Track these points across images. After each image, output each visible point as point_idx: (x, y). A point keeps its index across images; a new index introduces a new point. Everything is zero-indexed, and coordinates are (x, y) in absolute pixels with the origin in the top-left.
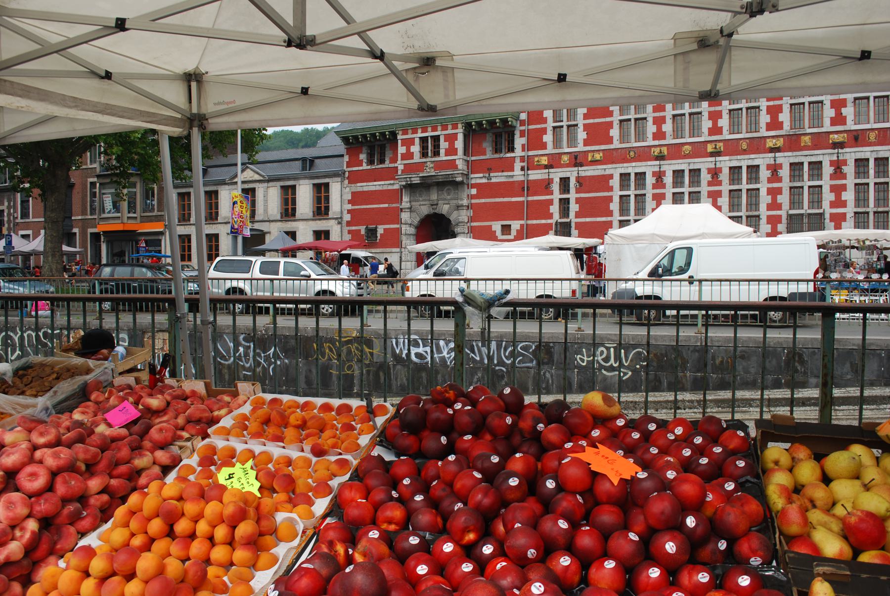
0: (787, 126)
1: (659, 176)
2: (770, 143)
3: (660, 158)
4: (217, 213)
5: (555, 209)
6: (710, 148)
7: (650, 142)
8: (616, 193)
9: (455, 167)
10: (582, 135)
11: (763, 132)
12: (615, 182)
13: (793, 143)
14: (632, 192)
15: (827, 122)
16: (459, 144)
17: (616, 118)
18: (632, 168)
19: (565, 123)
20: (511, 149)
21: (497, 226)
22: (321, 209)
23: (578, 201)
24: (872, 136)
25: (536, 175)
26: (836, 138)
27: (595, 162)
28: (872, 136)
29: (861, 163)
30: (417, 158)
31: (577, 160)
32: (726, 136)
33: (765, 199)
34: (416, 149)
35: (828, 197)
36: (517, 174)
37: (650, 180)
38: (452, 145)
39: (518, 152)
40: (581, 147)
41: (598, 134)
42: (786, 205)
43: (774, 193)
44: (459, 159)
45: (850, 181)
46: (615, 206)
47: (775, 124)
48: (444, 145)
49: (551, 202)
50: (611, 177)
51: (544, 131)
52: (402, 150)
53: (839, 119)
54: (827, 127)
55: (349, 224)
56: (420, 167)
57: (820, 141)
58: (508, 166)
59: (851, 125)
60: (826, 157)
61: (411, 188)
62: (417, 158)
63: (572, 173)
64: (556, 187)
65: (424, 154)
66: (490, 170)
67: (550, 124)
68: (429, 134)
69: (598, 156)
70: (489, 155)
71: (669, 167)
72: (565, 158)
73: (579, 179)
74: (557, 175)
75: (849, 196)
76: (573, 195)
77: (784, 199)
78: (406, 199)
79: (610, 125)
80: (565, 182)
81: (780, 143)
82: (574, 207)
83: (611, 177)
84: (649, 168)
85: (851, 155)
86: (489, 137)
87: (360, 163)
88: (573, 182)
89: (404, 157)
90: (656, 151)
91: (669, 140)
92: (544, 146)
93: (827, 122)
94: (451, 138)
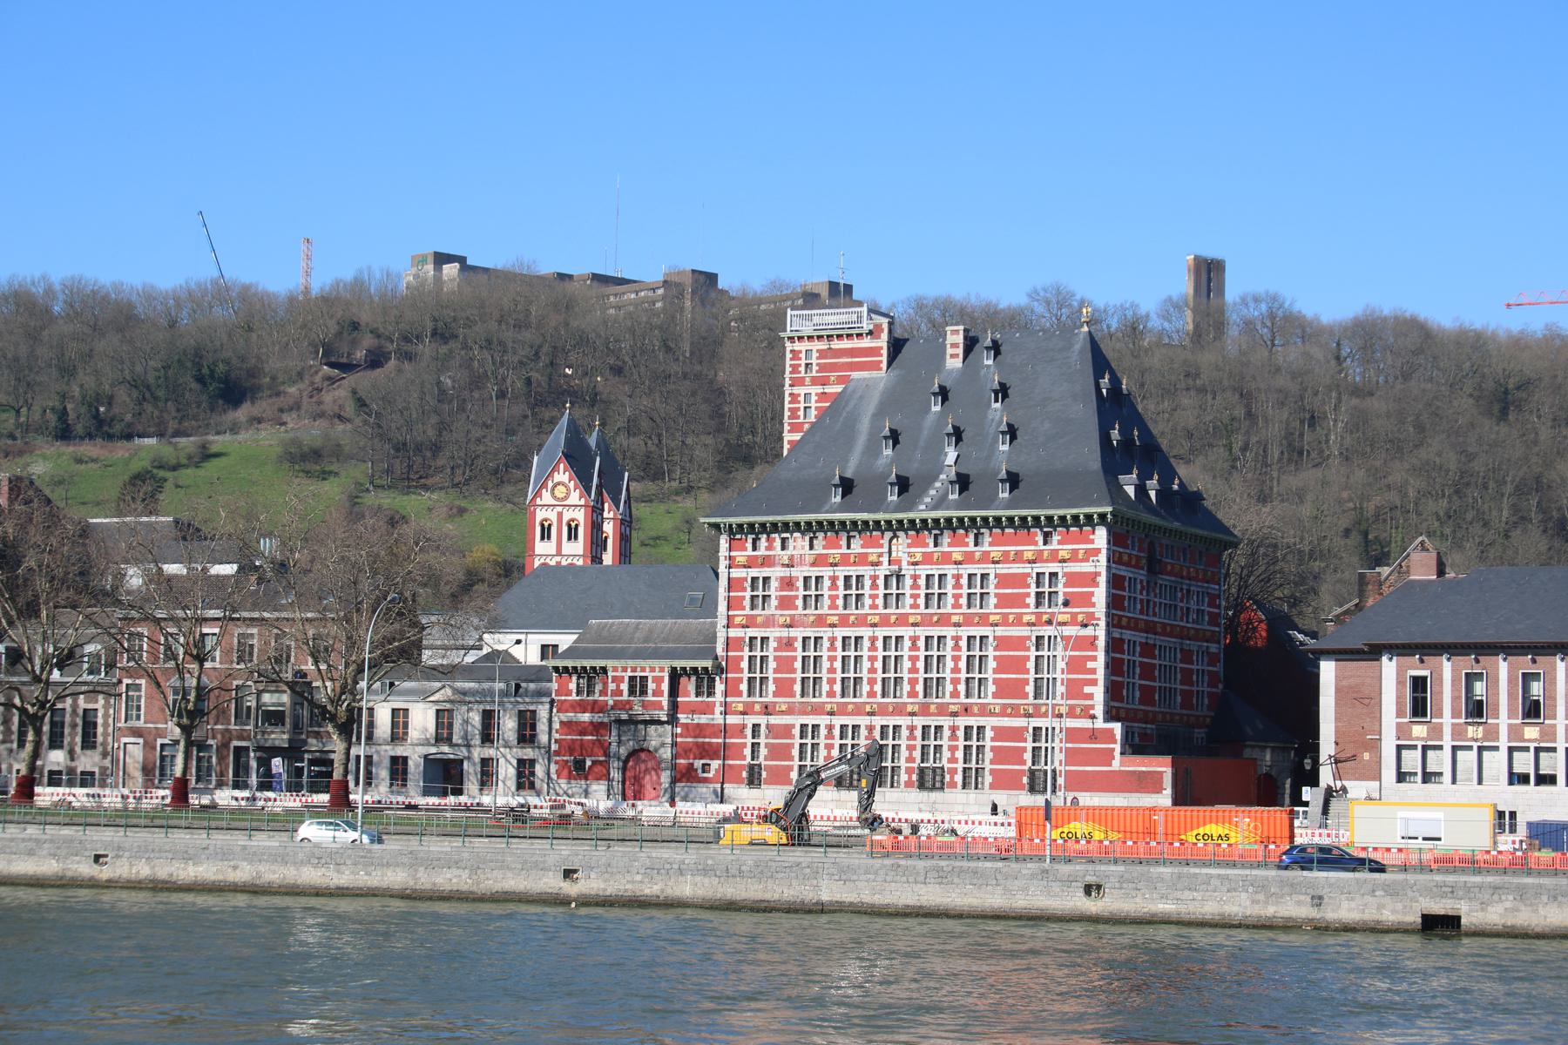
0: (921, 694)
1: (830, 728)
2: (909, 709)
3: (832, 714)
4: (406, 734)
5: (748, 752)
6: (868, 709)
7: (824, 699)
8: (797, 741)
9: (661, 708)
10: (772, 687)
11: (905, 699)
12: (796, 732)
13: (924, 710)
14: (809, 741)
15: (948, 694)
16: (665, 686)
17: (799, 675)
18: (810, 720)
19: (758, 675)
20: (711, 693)
21: (698, 764)
22: (527, 734)
23: (767, 745)
24: (976, 710)
25: (732, 720)
26: (953, 708)
27: (782, 713)
28: (976, 710)
29: (968, 729)
30: (625, 697)
31: (767, 710)
32: (879, 699)
33: (904, 753)
34: (625, 687)
35: (946, 754)
36: (718, 718)
37: (823, 731)
38: (659, 686)
39: (719, 697)
40: (770, 699)
41: (784, 688)
42: (918, 760)
43: (911, 748)
44: (665, 700)
45: (961, 743)
46: (795, 752)
47: (913, 694)
48: (651, 686)
49: (744, 745)
50: (793, 726)
51: (741, 680)
52: (612, 686)
53: (955, 694)
54: (947, 699)
55: (557, 753)
56: (626, 706)
57: (942, 710)
58: (708, 709)
59: (962, 699)
60: (946, 722)
61: (619, 722)
62: (625, 697)
63: (762, 720)
64: (749, 732)
65: (632, 692)
66: (693, 712)
67: (746, 675)
68: (639, 674)
69: (784, 708)
70: (693, 698)
71: (838, 721)
72: (757, 708)
73: (768, 726)
74: (750, 720)
75: (960, 754)
76: (762, 740)
77: (917, 754)
78: (614, 732)
79: (794, 680)
80: (756, 727)
81: (916, 708)
82: (763, 751)
83: (793, 726)
84: (823, 721)
85: (962, 722)
86: (693, 679)
87: (569, 693)
88: (763, 728)
89: (614, 693)
90: (828, 708)
91: (838, 699)
92: (740, 694)
93: (948, 694)
94: (658, 680)
